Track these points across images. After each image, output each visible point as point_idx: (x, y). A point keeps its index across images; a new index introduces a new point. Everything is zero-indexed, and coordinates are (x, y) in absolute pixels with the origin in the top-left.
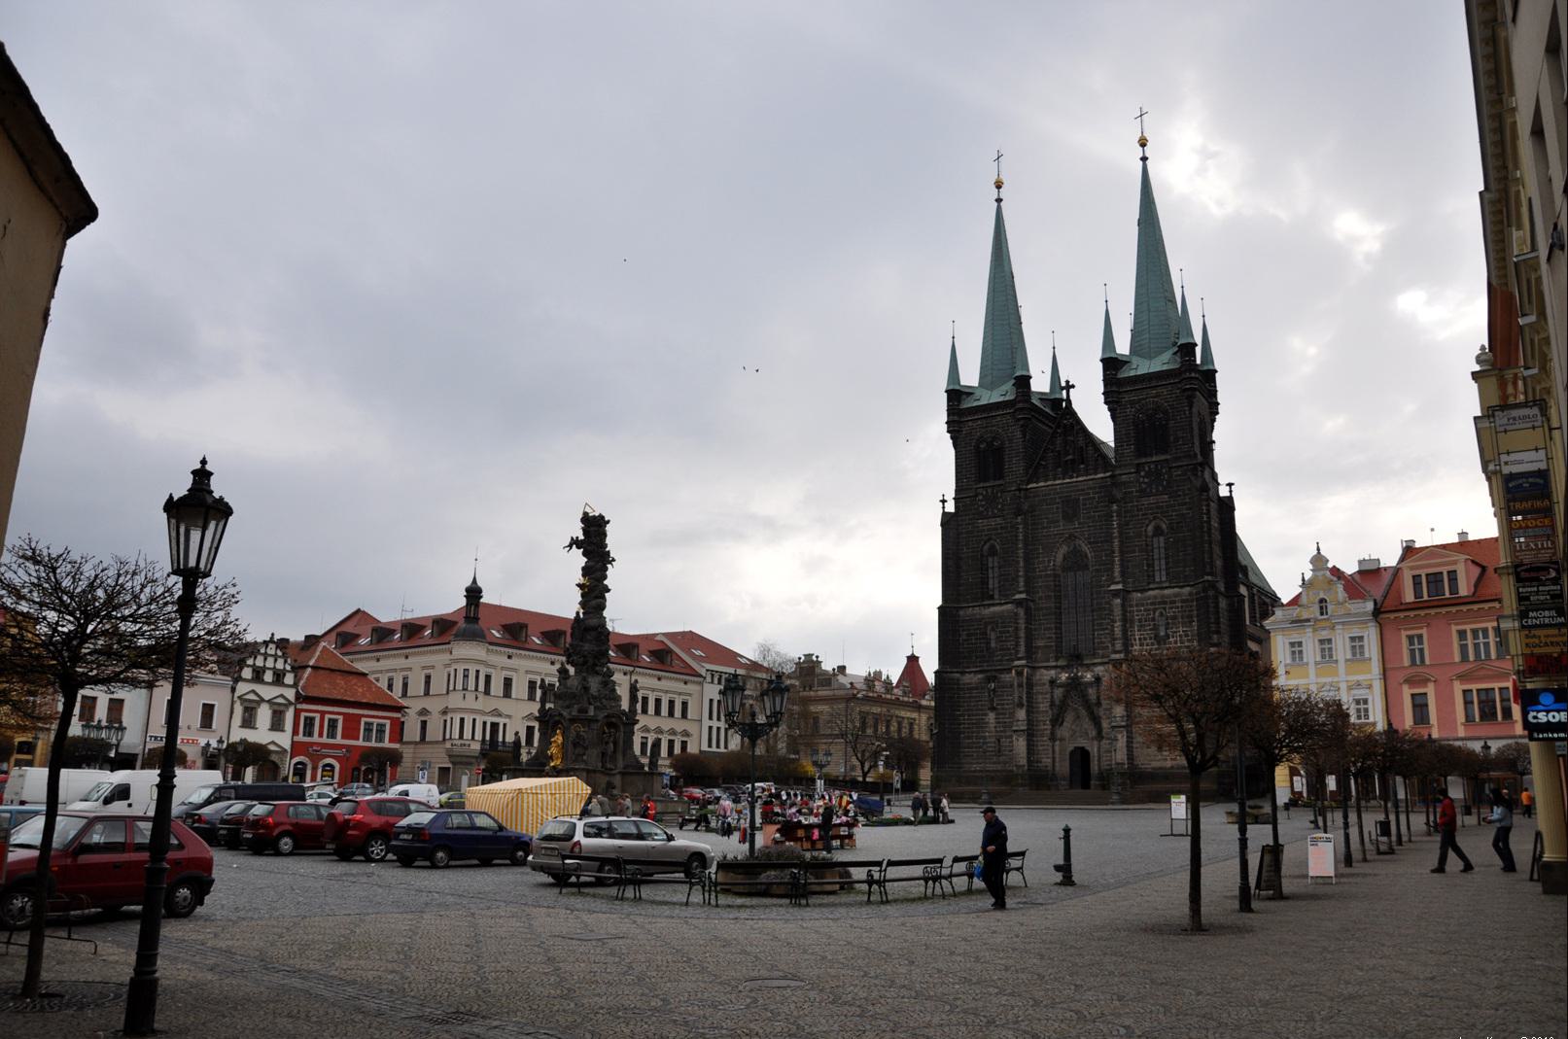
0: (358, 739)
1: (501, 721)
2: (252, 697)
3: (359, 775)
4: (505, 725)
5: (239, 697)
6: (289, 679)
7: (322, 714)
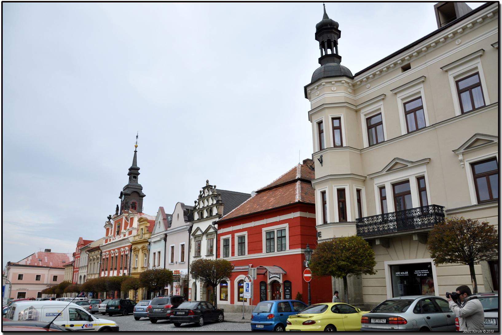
0: (260, 251)
1: (411, 175)
2: (199, 233)
3: (266, 289)
4: (420, 179)
5: (193, 235)
6: (215, 212)
7: (233, 233)
